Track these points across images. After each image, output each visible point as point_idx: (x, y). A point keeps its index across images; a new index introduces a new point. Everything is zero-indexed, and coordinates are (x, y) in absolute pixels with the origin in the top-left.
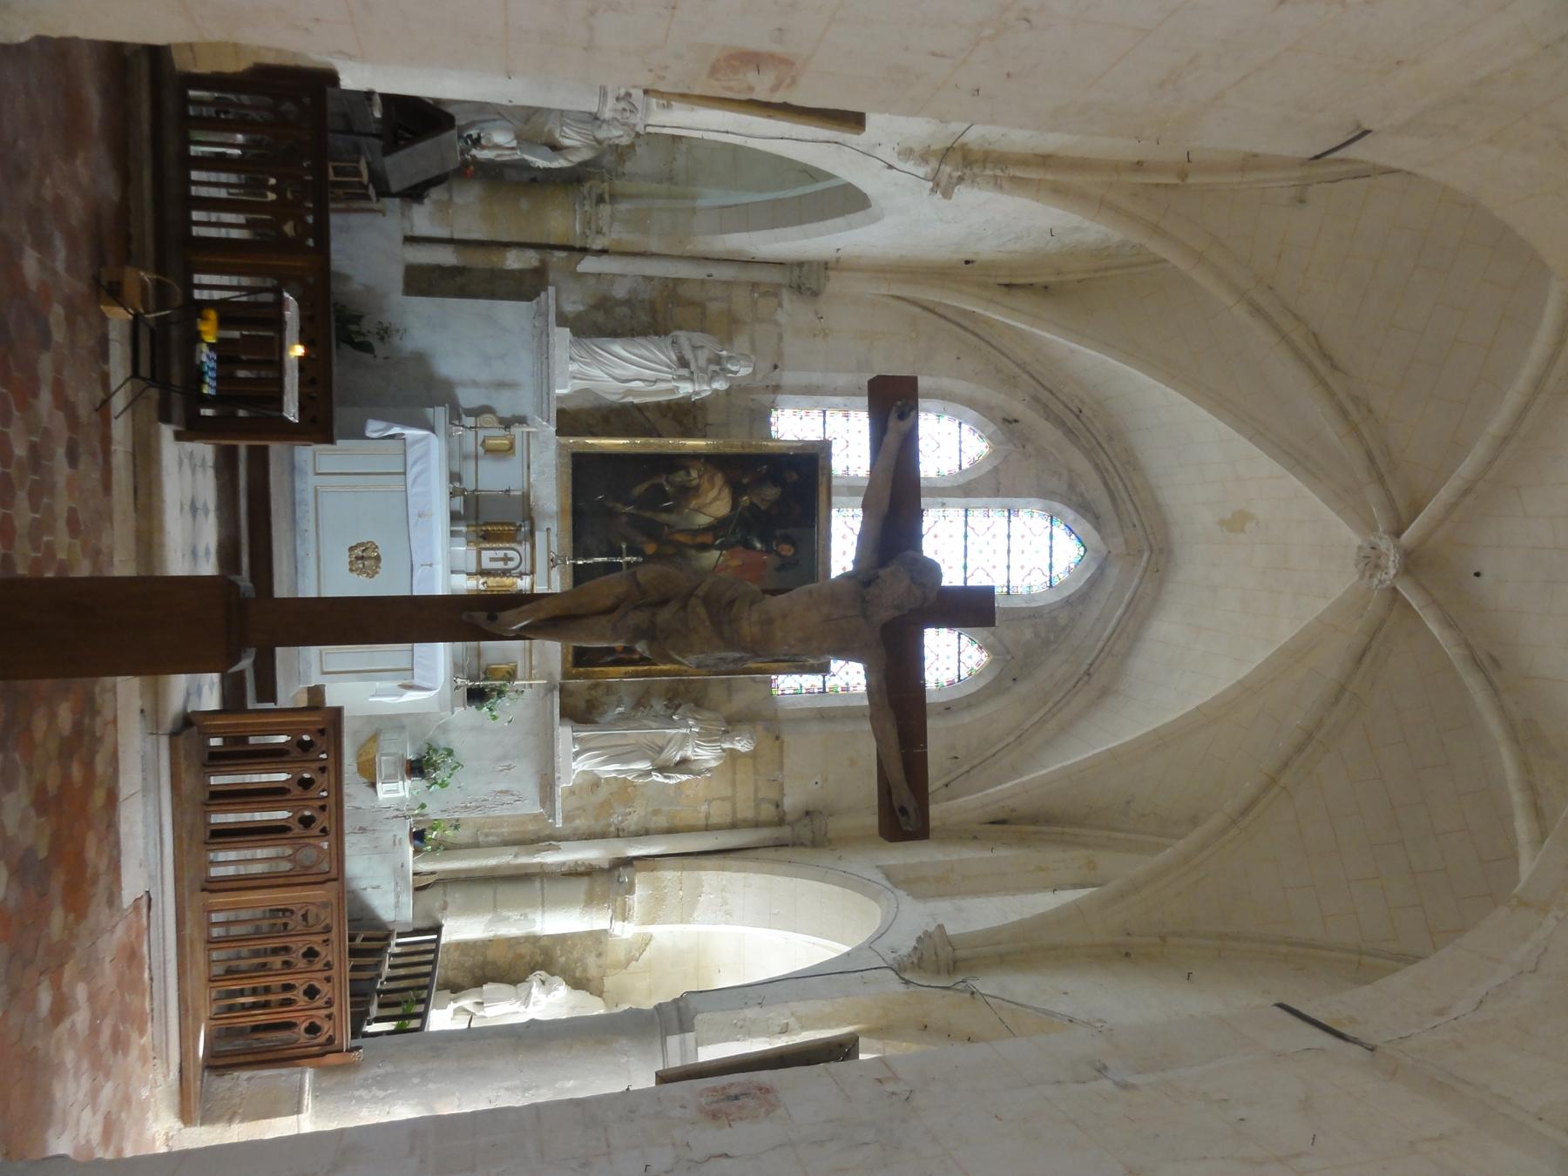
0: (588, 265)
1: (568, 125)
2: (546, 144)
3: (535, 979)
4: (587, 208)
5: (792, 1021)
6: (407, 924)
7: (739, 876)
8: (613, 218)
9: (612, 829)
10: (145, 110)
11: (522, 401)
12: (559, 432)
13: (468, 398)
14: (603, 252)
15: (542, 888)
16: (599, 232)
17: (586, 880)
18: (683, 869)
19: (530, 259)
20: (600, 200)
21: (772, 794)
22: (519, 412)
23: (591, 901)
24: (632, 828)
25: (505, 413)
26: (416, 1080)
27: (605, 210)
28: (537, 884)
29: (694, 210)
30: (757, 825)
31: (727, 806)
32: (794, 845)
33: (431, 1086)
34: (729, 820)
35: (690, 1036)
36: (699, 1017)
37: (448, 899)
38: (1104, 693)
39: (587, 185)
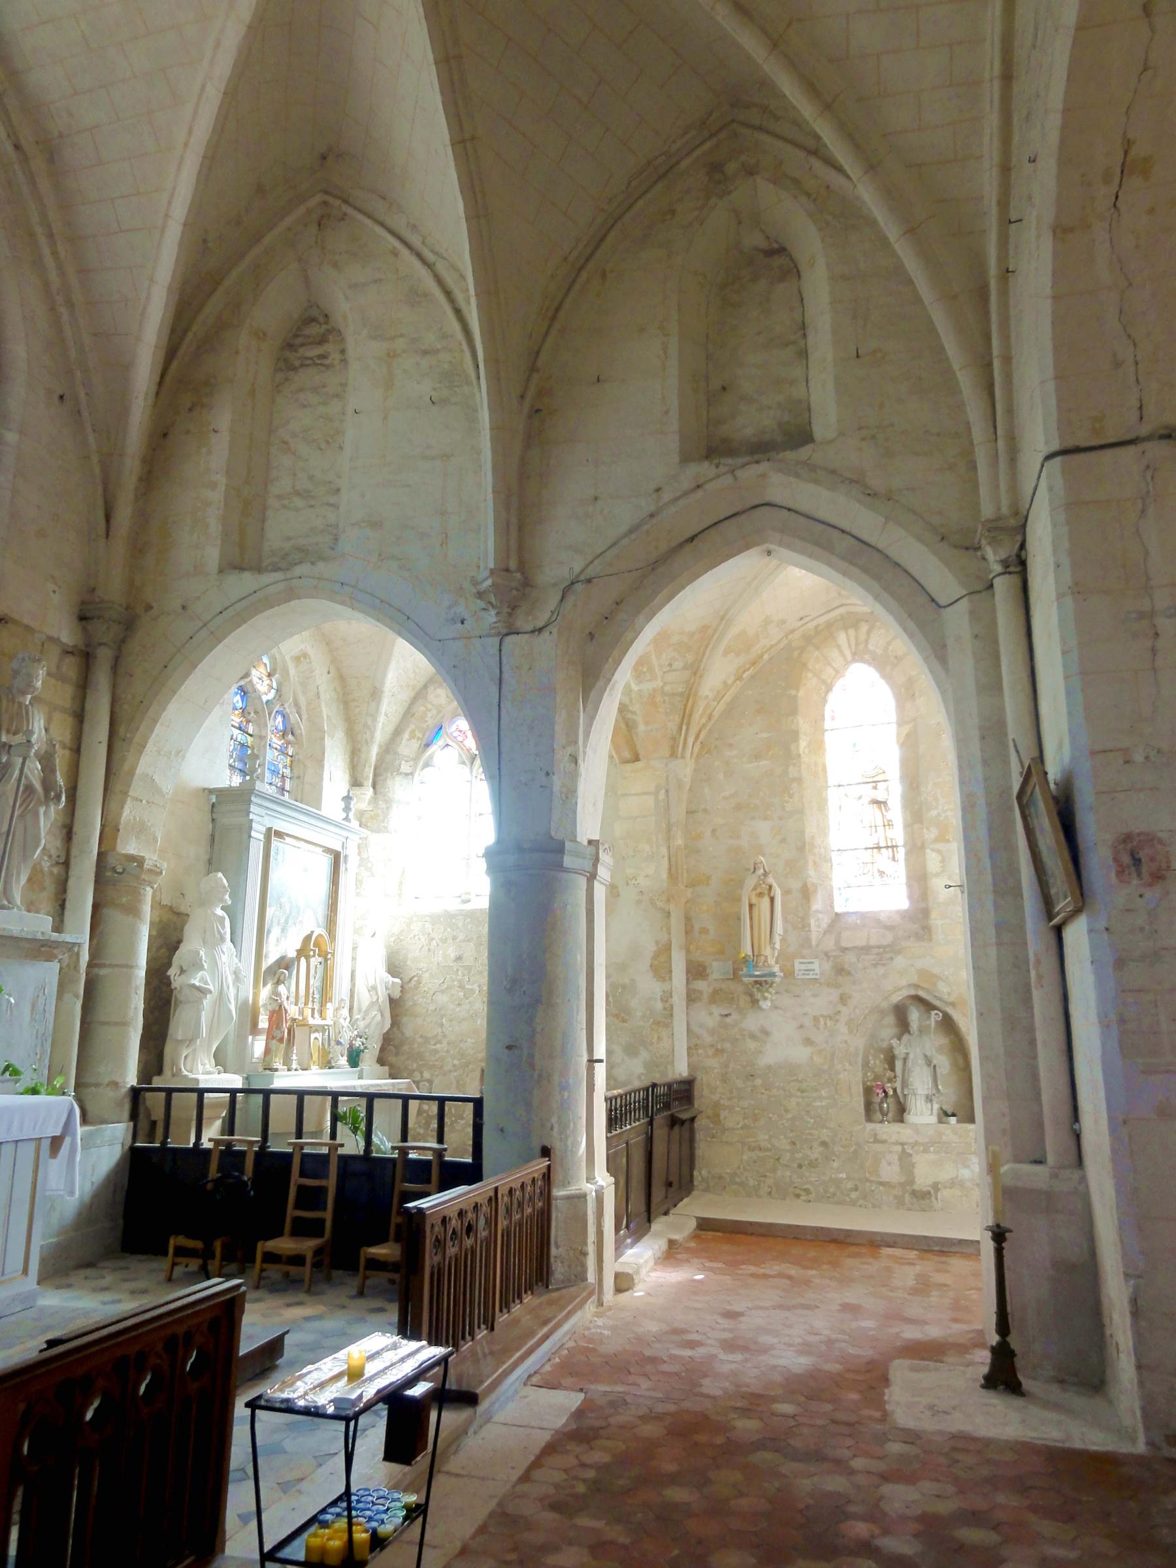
3: (177, 981)
5: (570, 750)
6: (127, 1129)
7: (158, 729)
9: (55, 870)
15: (111, 966)
17: (109, 913)
18: (125, 794)
21: (54, 652)
23: (133, 910)
24: (58, 843)
26: (566, 1094)
28: (102, 972)
30: (84, 686)
31: (57, 716)
32: (119, 649)
33: (571, 1081)
34: (69, 721)
35: (568, 845)
36: (553, 834)
37: (106, 1081)
38: (51, 151)
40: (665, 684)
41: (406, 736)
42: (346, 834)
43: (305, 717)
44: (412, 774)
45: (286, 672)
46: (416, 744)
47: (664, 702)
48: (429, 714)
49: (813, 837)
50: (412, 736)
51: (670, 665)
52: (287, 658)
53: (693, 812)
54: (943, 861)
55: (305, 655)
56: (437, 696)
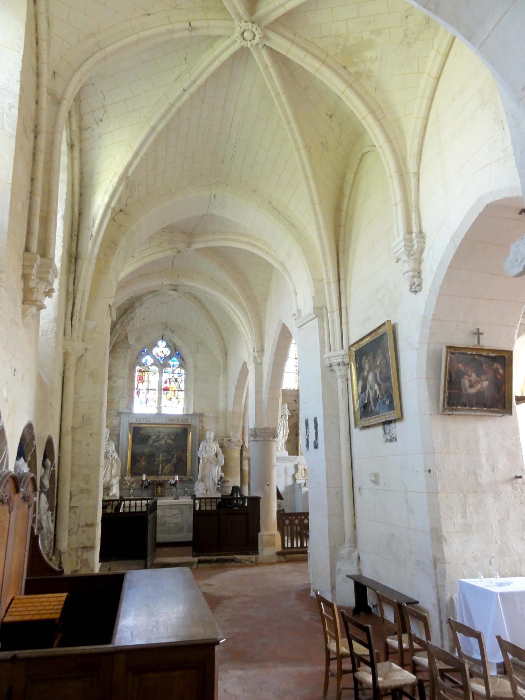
0: (247, 444)
1: (211, 450)
2: (217, 457)
4: (232, 445)
8: (235, 437)
10: (299, 555)
11: (290, 466)
12: (298, 455)
13: (290, 482)
14: (243, 439)
16: (239, 441)
19: (246, 462)
20: (230, 441)
22: (293, 467)
25: (293, 471)
27: (233, 439)
29: (233, 412)
39: (225, 444)
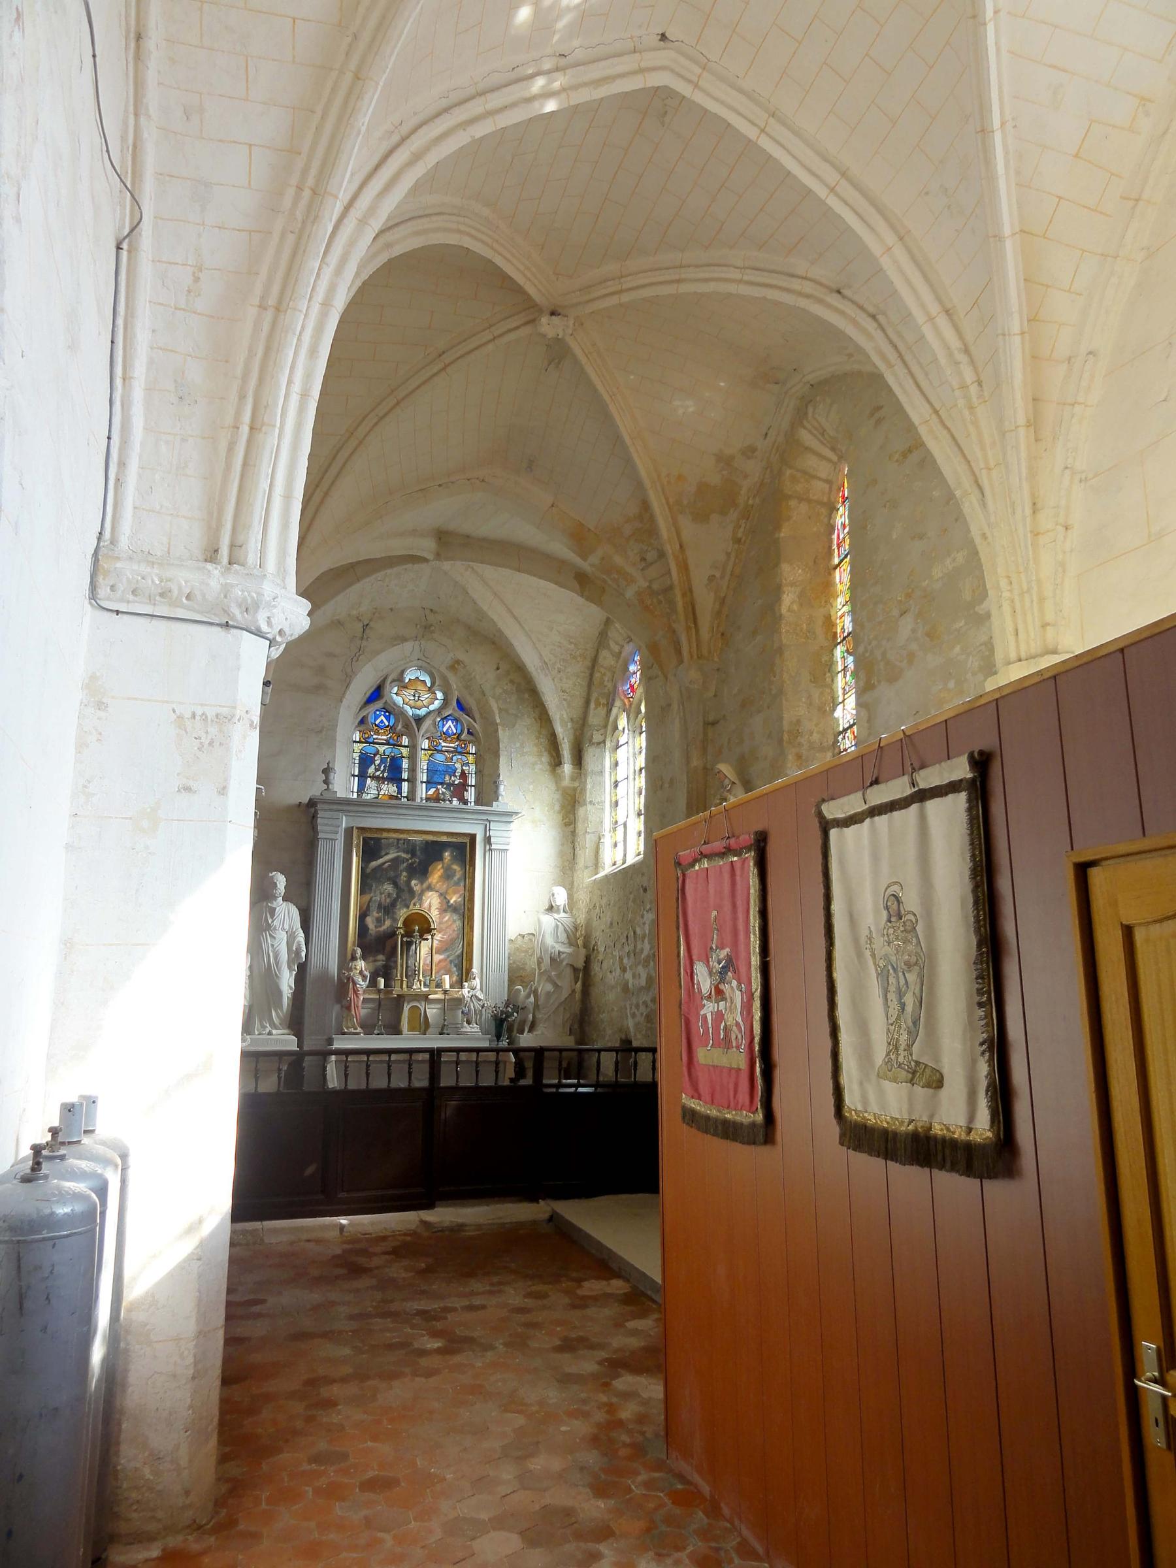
40: (651, 582)
41: (592, 705)
42: (485, 817)
43: (477, 716)
44: (604, 742)
45: (445, 681)
46: (602, 711)
47: (660, 602)
48: (606, 679)
49: (798, 722)
50: (598, 704)
51: (643, 559)
52: (443, 669)
53: (713, 724)
54: (869, 721)
55: (458, 662)
56: (605, 658)
